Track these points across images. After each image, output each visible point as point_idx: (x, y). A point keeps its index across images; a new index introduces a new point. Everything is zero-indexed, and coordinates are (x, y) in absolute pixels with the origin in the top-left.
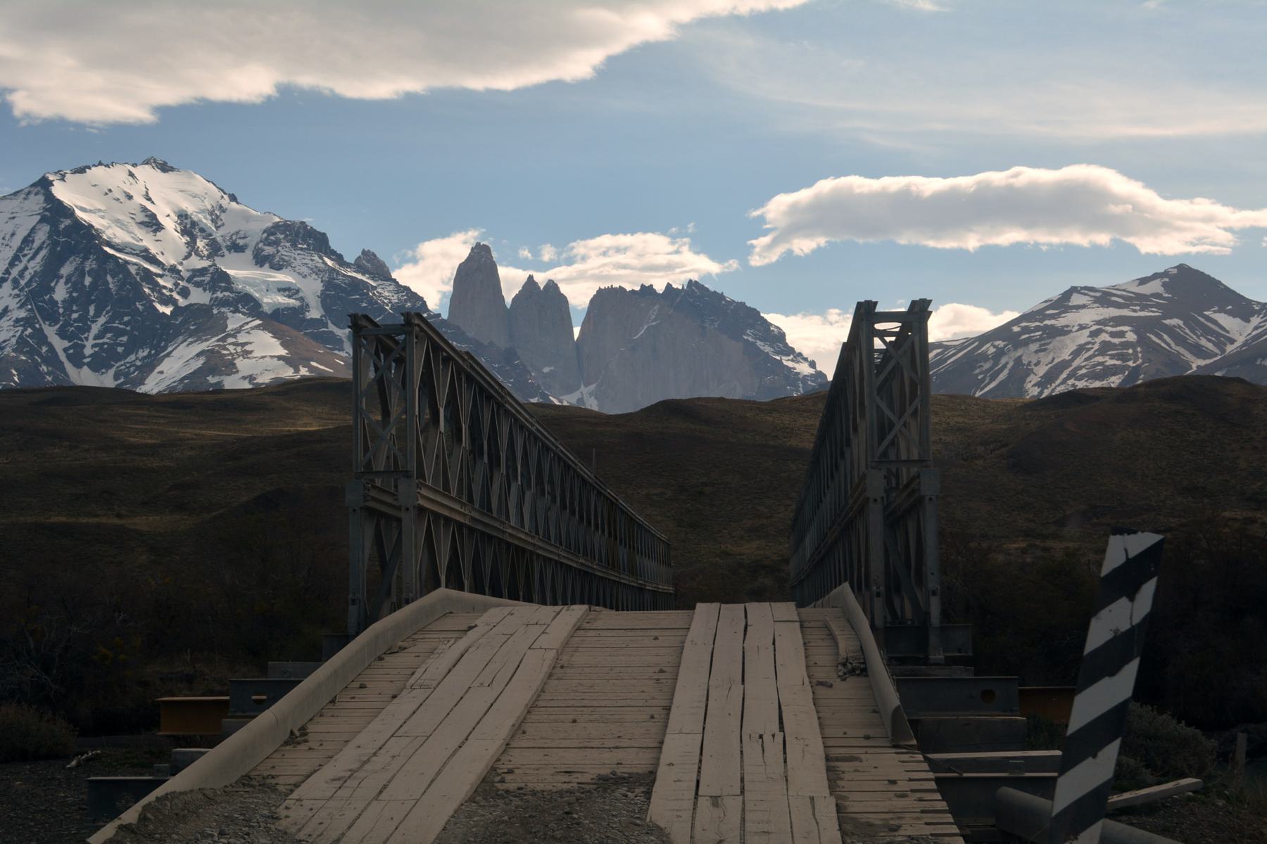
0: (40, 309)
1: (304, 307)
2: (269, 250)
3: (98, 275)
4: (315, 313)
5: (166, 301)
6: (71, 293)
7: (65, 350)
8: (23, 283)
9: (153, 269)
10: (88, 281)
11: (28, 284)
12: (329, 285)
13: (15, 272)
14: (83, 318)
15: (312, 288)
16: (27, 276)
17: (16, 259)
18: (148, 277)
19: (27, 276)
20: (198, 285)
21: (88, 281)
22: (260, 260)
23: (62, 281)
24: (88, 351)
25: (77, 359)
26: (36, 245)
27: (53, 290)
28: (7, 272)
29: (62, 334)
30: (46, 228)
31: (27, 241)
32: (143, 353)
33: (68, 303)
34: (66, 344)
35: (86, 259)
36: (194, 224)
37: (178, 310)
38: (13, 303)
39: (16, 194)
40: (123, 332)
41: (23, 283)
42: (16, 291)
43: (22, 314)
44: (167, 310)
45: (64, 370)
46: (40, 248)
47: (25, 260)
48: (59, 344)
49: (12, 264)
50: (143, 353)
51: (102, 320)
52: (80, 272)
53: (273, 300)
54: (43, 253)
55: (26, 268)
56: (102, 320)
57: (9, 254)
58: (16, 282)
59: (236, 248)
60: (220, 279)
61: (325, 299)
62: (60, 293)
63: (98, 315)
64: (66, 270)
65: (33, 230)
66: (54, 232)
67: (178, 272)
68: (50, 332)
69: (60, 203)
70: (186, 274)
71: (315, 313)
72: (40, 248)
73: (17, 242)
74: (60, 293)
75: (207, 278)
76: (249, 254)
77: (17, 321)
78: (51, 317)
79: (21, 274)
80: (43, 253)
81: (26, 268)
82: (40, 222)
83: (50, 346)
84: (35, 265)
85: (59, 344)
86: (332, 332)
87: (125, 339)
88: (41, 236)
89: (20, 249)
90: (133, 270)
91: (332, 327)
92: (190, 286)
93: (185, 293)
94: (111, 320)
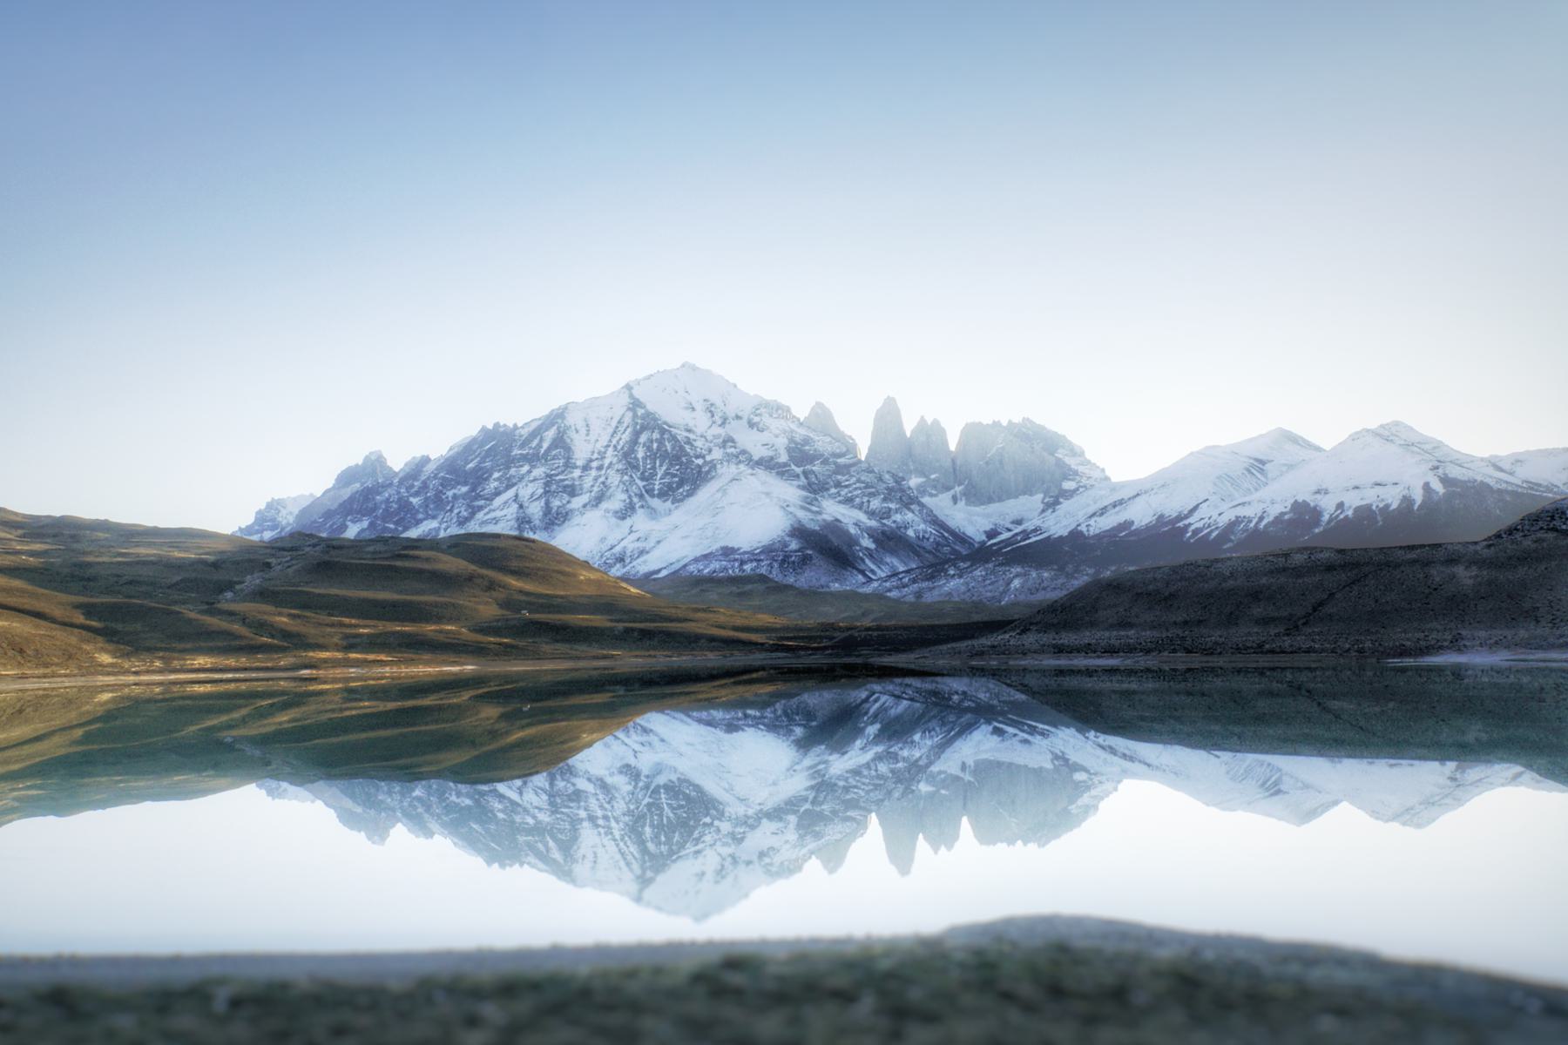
1: (778, 455)
2: (756, 419)
3: (661, 442)
4: (784, 458)
9: (692, 436)
12: (792, 440)
14: (654, 468)
15: (782, 443)
18: (689, 442)
21: (655, 445)
22: (751, 425)
25: (650, 492)
29: (642, 479)
30: (630, 414)
33: (645, 459)
40: (674, 476)
43: (620, 466)
44: (700, 461)
57: (610, 430)
59: (738, 417)
60: (728, 441)
61: (789, 450)
62: (641, 454)
64: (643, 438)
66: (635, 416)
71: (784, 458)
73: (614, 424)
74: (641, 454)
76: (745, 421)
78: (636, 467)
84: (626, 437)
88: (628, 419)
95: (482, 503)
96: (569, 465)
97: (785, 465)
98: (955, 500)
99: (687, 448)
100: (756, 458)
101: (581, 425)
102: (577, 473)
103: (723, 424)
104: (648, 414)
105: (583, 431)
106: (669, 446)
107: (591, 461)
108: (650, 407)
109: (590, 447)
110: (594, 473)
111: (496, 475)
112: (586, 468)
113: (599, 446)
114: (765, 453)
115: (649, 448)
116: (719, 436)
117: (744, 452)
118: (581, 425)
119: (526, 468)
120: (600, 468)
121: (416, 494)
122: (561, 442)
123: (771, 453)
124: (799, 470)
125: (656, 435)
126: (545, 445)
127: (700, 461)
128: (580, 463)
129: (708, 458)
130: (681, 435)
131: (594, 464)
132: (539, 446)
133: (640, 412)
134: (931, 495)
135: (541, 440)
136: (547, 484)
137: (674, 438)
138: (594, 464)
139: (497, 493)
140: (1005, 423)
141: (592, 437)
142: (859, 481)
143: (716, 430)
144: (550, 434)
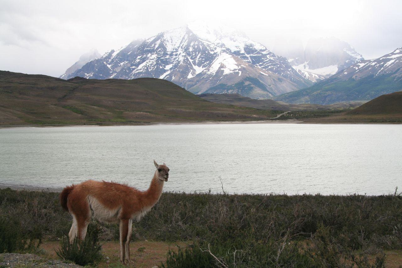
0: (187, 53)
4: (243, 52)
5: (213, 51)
7: (192, 62)
9: (209, 43)
13: (181, 45)
17: (181, 42)
20: (218, 46)
24: (197, 62)
25: (194, 63)
28: (180, 45)
29: (192, 58)
30: (187, 35)
32: (208, 62)
34: (192, 60)
37: (215, 53)
38: (182, 52)
40: (203, 58)
43: (184, 54)
45: (192, 66)
48: (191, 61)
49: (181, 43)
50: (208, 62)
51: (199, 55)
53: (233, 49)
56: (199, 55)
57: (180, 41)
58: (182, 47)
61: (245, 49)
63: (198, 54)
65: (185, 36)
67: (214, 44)
68: (189, 58)
70: (216, 44)
75: (220, 45)
77: (183, 56)
78: (189, 55)
83: (190, 62)
84: (185, 44)
85: (191, 61)
86: (246, 56)
87: (204, 59)
88: (186, 37)
89: (182, 40)
90: (205, 44)
91: (246, 55)
93: (215, 49)
94: (201, 55)
95: (134, 67)
96: (165, 54)
97: (243, 54)
98: (305, 66)
99: (208, 48)
100: (233, 51)
102: (168, 57)
103: (220, 39)
104: (193, 35)
105: (170, 41)
106: (201, 47)
107: (173, 52)
108: (195, 33)
110: (174, 57)
111: (139, 57)
112: (171, 55)
113: (176, 47)
114: (236, 50)
115: (194, 48)
116: (219, 44)
117: (228, 49)
118: (169, 39)
119: (150, 54)
120: (176, 55)
121: (109, 64)
122: (162, 46)
123: (239, 50)
124: (248, 56)
125: (196, 43)
126: (157, 46)
127: (212, 53)
128: (169, 53)
129: (215, 51)
130: (206, 43)
131: (174, 54)
132: (154, 47)
134: (296, 65)
135: (155, 45)
136: (157, 61)
137: (203, 44)
138: (174, 54)
139: (139, 63)
142: (270, 60)
143: (218, 41)
144: (158, 42)
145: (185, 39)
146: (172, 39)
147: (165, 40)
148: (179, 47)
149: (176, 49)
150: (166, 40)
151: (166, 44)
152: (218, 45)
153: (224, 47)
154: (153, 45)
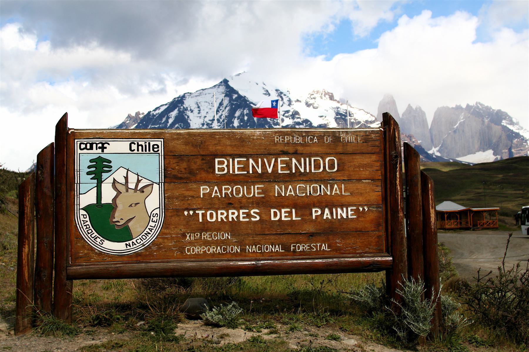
6: (240, 123)
8: (221, 120)
10: (246, 118)
11: (223, 121)
16: (223, 117)
19: (223, 117)
20: (287, 117)
21: (246, 118)
23: (236, 119)
26: (225, 105)
27: (233, 122)
31: (221, 104)
35: (244, 109)
36: (281, 93)
39: (215, 86)
41: (221, 120)
42: (219, 124)
46: (226, 107)
47: (221, 111)
52: (242, 115)
54: (228, 108)
55: (222, 115)
58: (218, 120)
62: (236, 123)
64: (237, 114)
66: (231, 100)
69: (232, 89)
72: (226, 107)
74: (236, 123)
75: (290, 113)
79: (220, 117)
80: (228, 108)
81: (222, 115)
82: (225, 96)
88: (226, 102)
89: (219, 107)
92: (284, 118)
101: (194, 107)
105: (196, 111)
108: (242, 93)
109: (201, 121)
116: (288, 112)
118: (194, 107)
126: (171, 121)
132: (167, 121)
133: (235, 96)
135: (168, 118)
140: (464, 106)
141: (203, 114)
144: (174, 114)
145: (225, 105)
146: (199, 107)
147: (186, 109)
148: (213, 120)
149: (208, 124)
150: (189, 109)
151: (188, 117)
152: (286, 115)
153: (298, 118)
154: (164, 120)
